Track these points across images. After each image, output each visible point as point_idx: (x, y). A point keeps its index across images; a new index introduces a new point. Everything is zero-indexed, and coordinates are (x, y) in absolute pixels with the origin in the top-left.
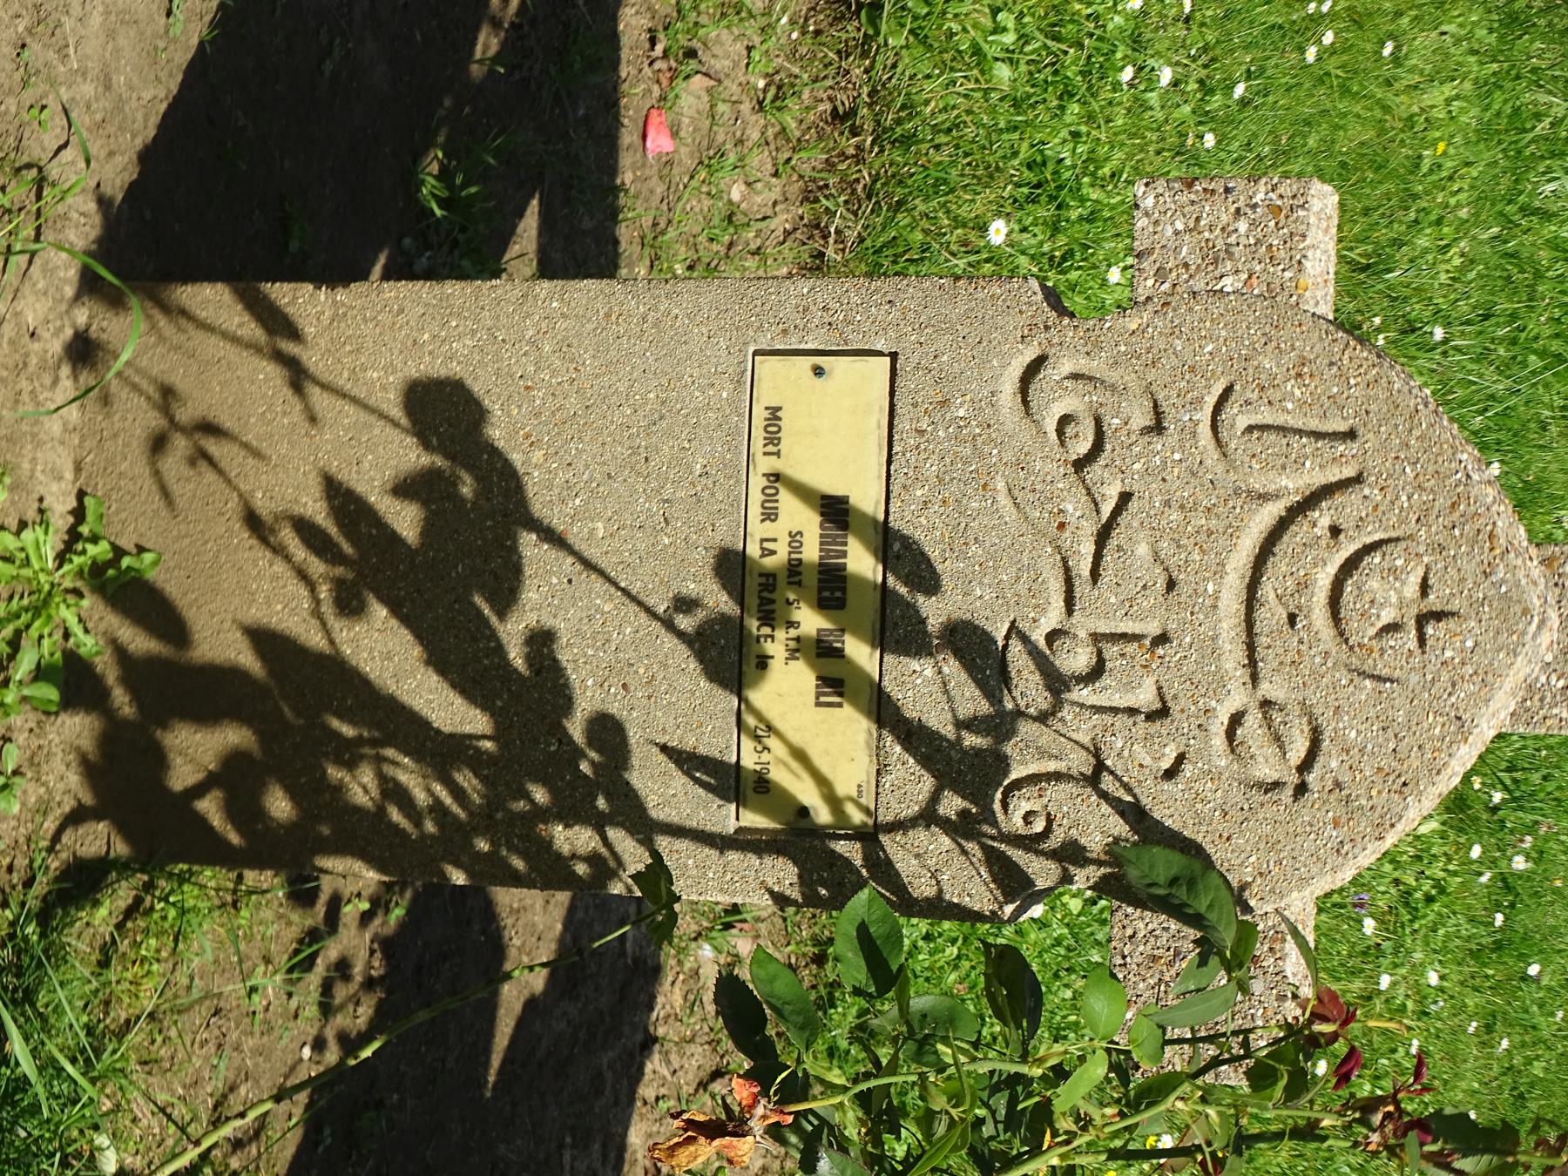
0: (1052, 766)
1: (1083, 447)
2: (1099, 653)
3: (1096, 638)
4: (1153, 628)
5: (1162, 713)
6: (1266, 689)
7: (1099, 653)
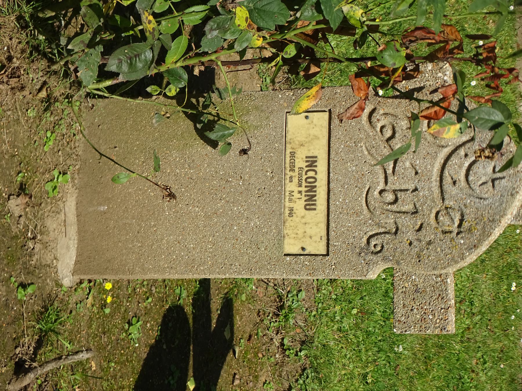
0: (382, 230)
1: (388, 133)
2: (396, 195)
3: (395, 191)
4: (411, 187)
5: (416, 212)
6: (447, 202)
7: (396, 195)
